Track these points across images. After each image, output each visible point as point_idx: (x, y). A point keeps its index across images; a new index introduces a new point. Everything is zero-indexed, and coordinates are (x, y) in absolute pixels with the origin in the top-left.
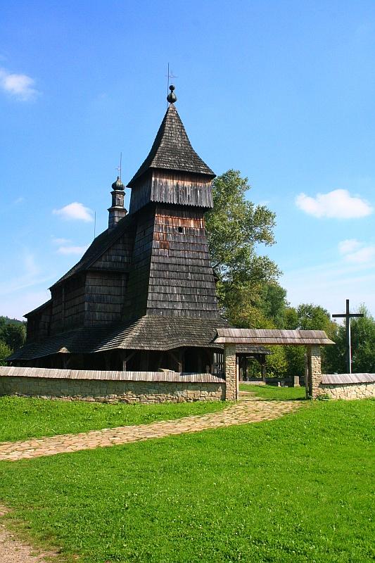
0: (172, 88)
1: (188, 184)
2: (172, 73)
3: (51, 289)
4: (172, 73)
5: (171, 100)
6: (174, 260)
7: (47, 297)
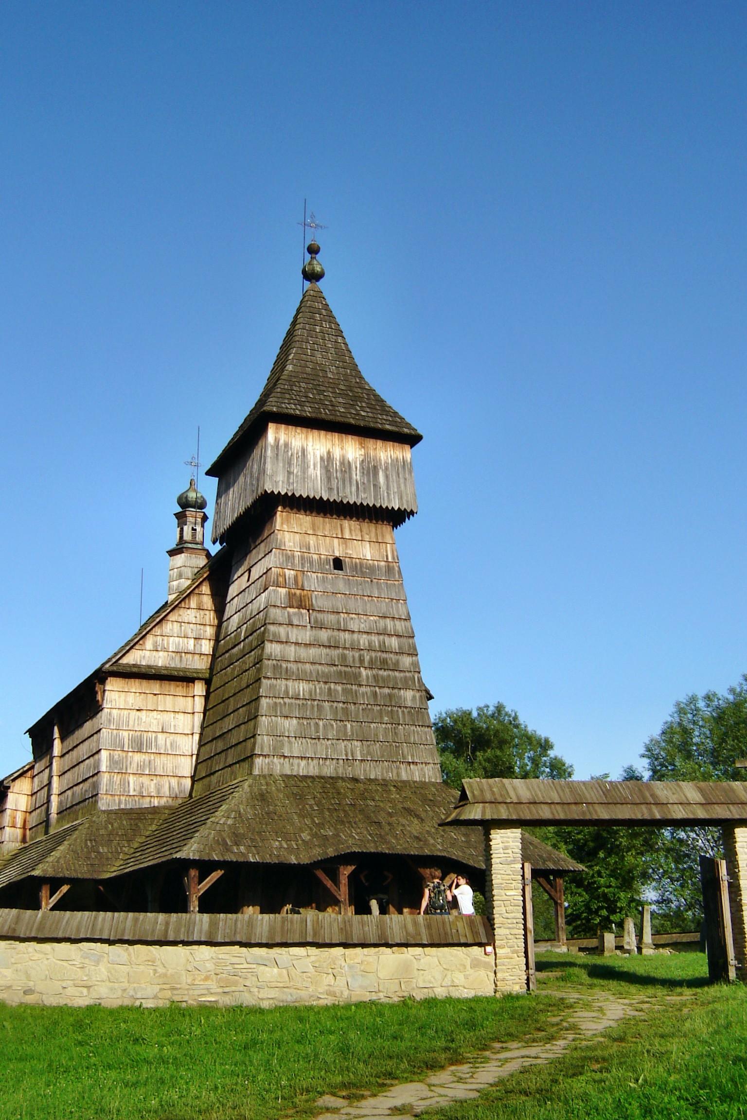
0: (313, 250)
2: (312, 217)
4: (312, 217)
5: (312, 276)
6: (324, 635)
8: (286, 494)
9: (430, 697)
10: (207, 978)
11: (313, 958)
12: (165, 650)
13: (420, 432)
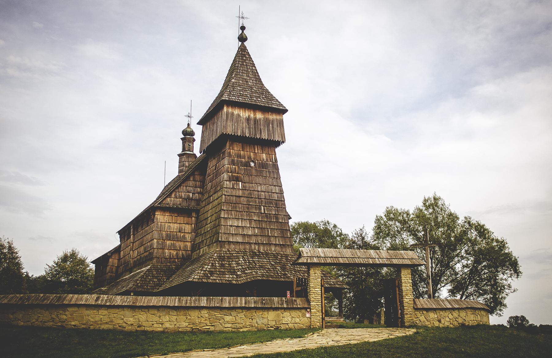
1: (259, 116)
3: (119, 232)
6: (246, 193)
7: (116, 241)
9: (290, 218)
10: (206, 320)
11: (244, 313)
12: (181, 197)
13: (287, 108)
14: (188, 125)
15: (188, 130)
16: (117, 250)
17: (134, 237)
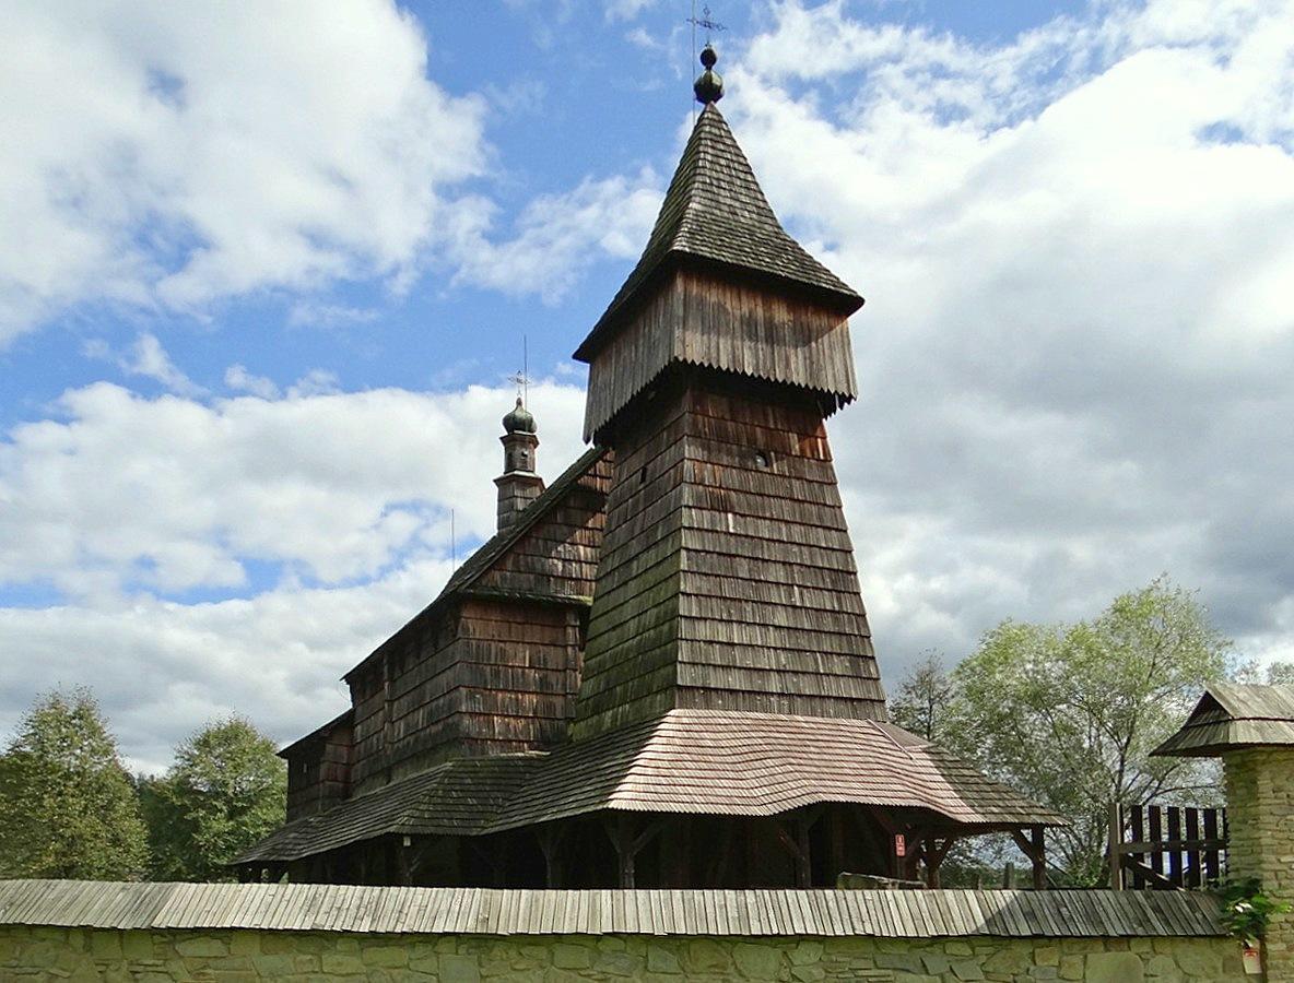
0: (708, 58)
8: (702, 364)
13: (860, 294)
14: (519, 403)
15: (519, 414)
16: (344, 723)
17: (391, 686)
